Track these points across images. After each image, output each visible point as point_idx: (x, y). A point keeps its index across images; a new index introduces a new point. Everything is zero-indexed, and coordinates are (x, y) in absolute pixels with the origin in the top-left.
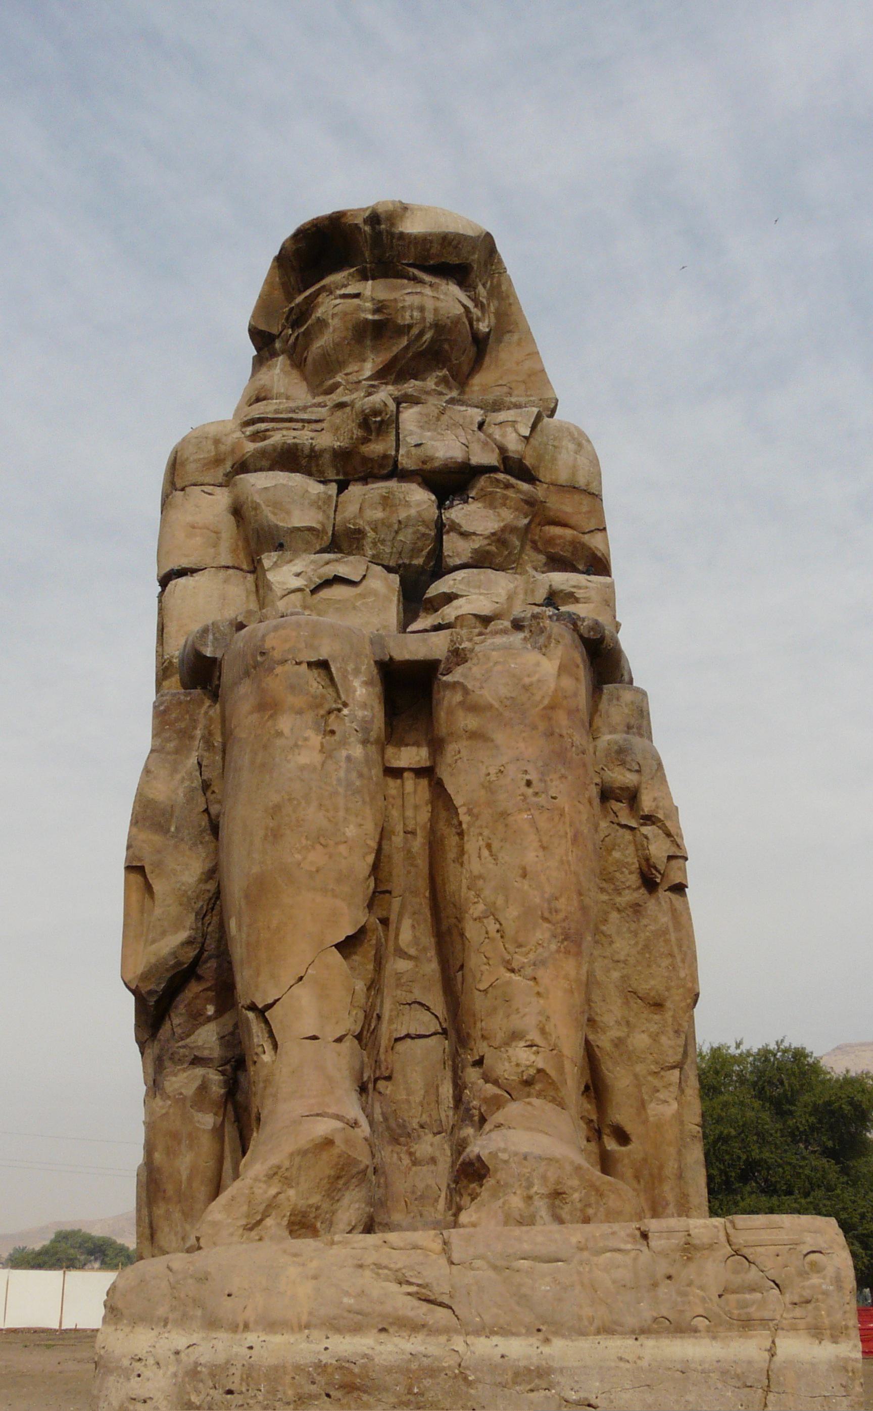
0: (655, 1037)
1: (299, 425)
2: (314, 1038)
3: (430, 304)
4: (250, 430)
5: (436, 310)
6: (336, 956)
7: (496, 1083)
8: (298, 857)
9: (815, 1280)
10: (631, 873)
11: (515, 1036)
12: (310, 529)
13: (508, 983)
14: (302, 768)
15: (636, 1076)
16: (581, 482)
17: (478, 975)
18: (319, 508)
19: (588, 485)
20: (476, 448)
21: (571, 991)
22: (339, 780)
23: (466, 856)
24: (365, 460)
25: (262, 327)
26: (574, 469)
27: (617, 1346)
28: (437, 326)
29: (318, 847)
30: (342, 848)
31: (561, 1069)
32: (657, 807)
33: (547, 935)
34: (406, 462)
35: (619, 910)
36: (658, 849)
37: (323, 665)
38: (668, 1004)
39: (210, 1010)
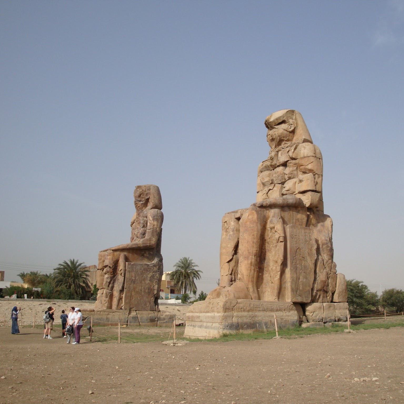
1: (267, 161)
3: (276, 133)
5: (278, 133)
6: (227, 264)
9: (218, 306)
10: (275, 241)
12: (267, 181)
16: (306, 155)
18: (268, 177)
19: (307, 155)
21: (246, 265)
22: (228, 239)
26: (304, 153)
27: (204, 314)
28: (279, 136)
29: (224, 249)
30: (228, 249)
31: (243, 277)
32: (277, 229)
33: (242, 258)
35: (274, 247)
37: (226, 222)
38: (278, 262)
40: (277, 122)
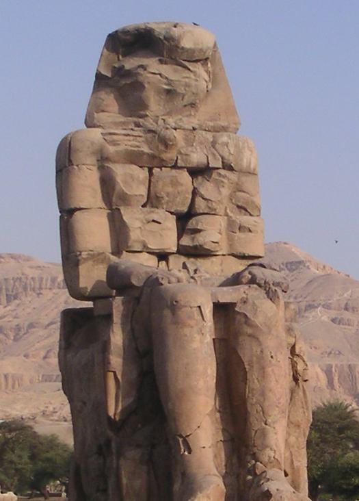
0: (297, 439)
1: (132, 138)
2: (204, 447)
3: (193, 83)
4: (107, 137)
7: (261, 463)
8: (196, 383)
11: (267, 447)
13: (264, 429)
14: (194, 349)
15: (291, 452)
16: (252, 171)
17: (253, 424)
20: (210, 158)
23: (248, 381)
24: (163, 160)
25: (104, 72)
34: (180, 163)
36: (300, 367)
37: (199, 307)
38: (302, 426)
39: (139, 426)
40: (197, 56)
